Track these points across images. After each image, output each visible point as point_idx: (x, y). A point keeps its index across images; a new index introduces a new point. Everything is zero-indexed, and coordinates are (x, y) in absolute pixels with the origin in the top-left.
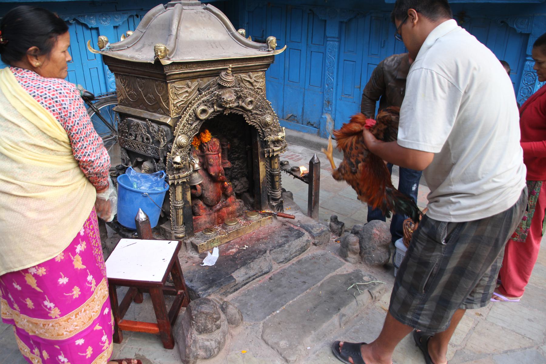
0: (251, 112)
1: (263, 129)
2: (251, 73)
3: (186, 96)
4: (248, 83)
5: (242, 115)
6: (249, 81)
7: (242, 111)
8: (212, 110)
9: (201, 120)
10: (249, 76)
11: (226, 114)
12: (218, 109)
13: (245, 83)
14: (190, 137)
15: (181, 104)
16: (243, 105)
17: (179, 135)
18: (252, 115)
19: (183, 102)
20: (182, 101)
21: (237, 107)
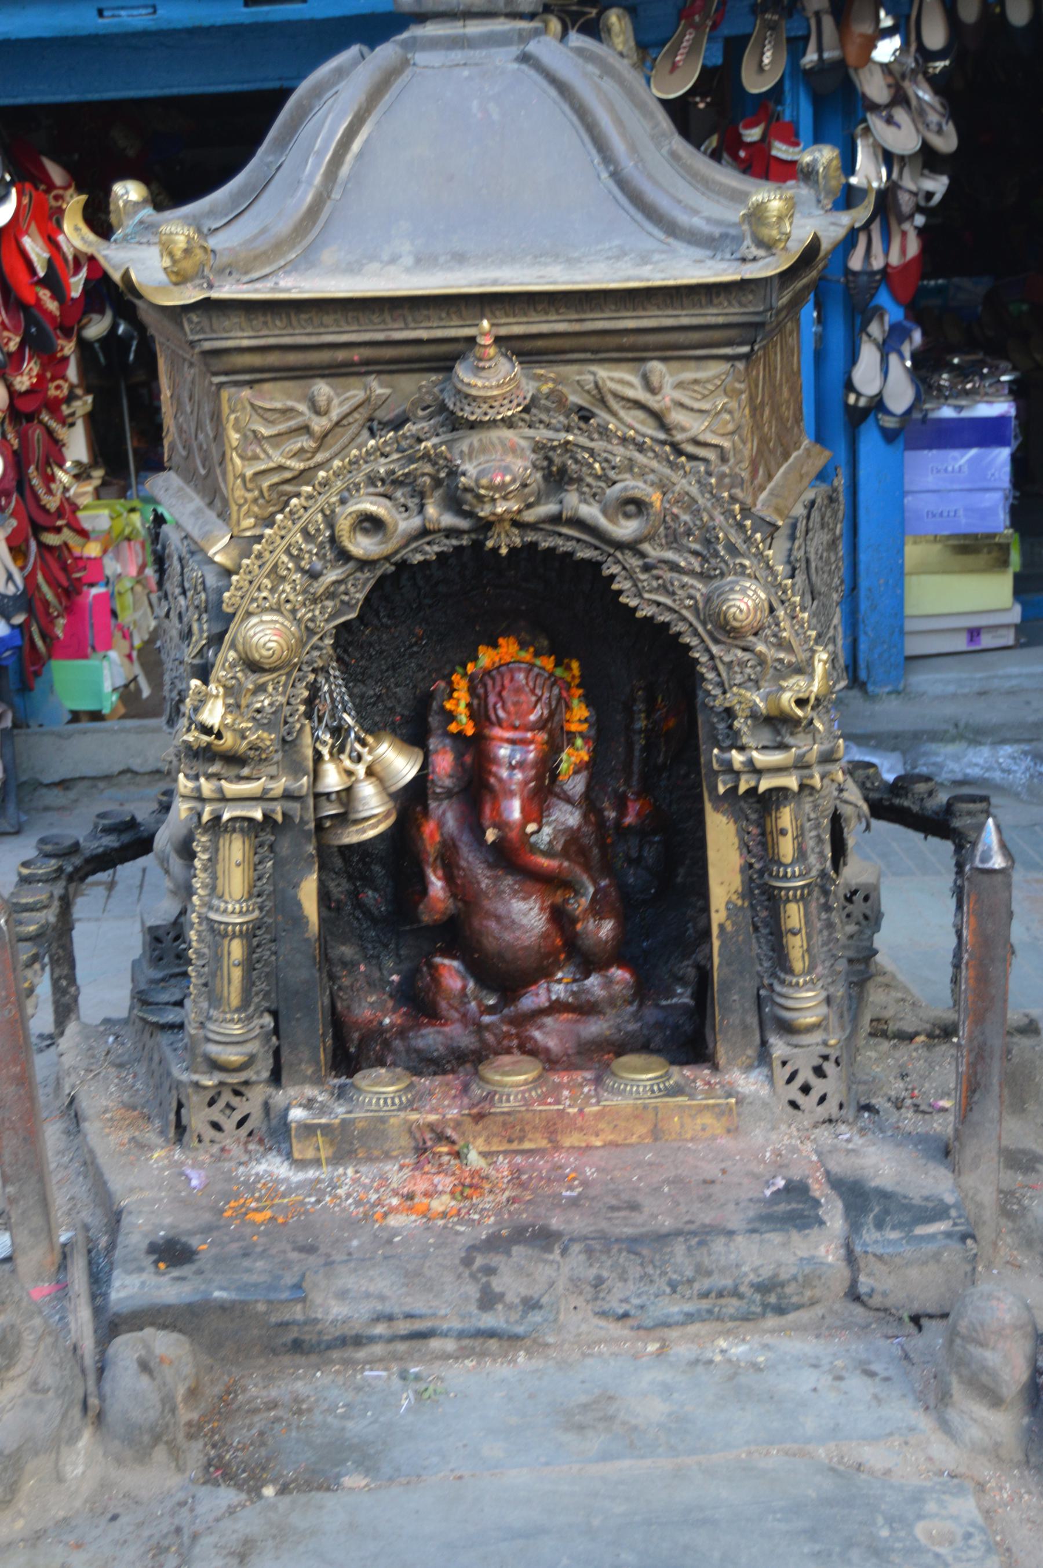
0: (643, 555)
1: (715, 649)
2: (656, 367)
3: (302, 450)
4: (640, 414)
5: (596, 566)
6: (638, 405)
7: (596, 548)
8: (416, 522)
9: (364, 564)
10: (646, 380)
11: (495, 550)
12: (448, 520)
13: (622, 413)
14: (311, 632)
15: (275, 479)
16: (590, 511)
17: (249, 614)
18: (647, 568)
19: (288, 475)
20: (281, 468)
21: (556, 519)
